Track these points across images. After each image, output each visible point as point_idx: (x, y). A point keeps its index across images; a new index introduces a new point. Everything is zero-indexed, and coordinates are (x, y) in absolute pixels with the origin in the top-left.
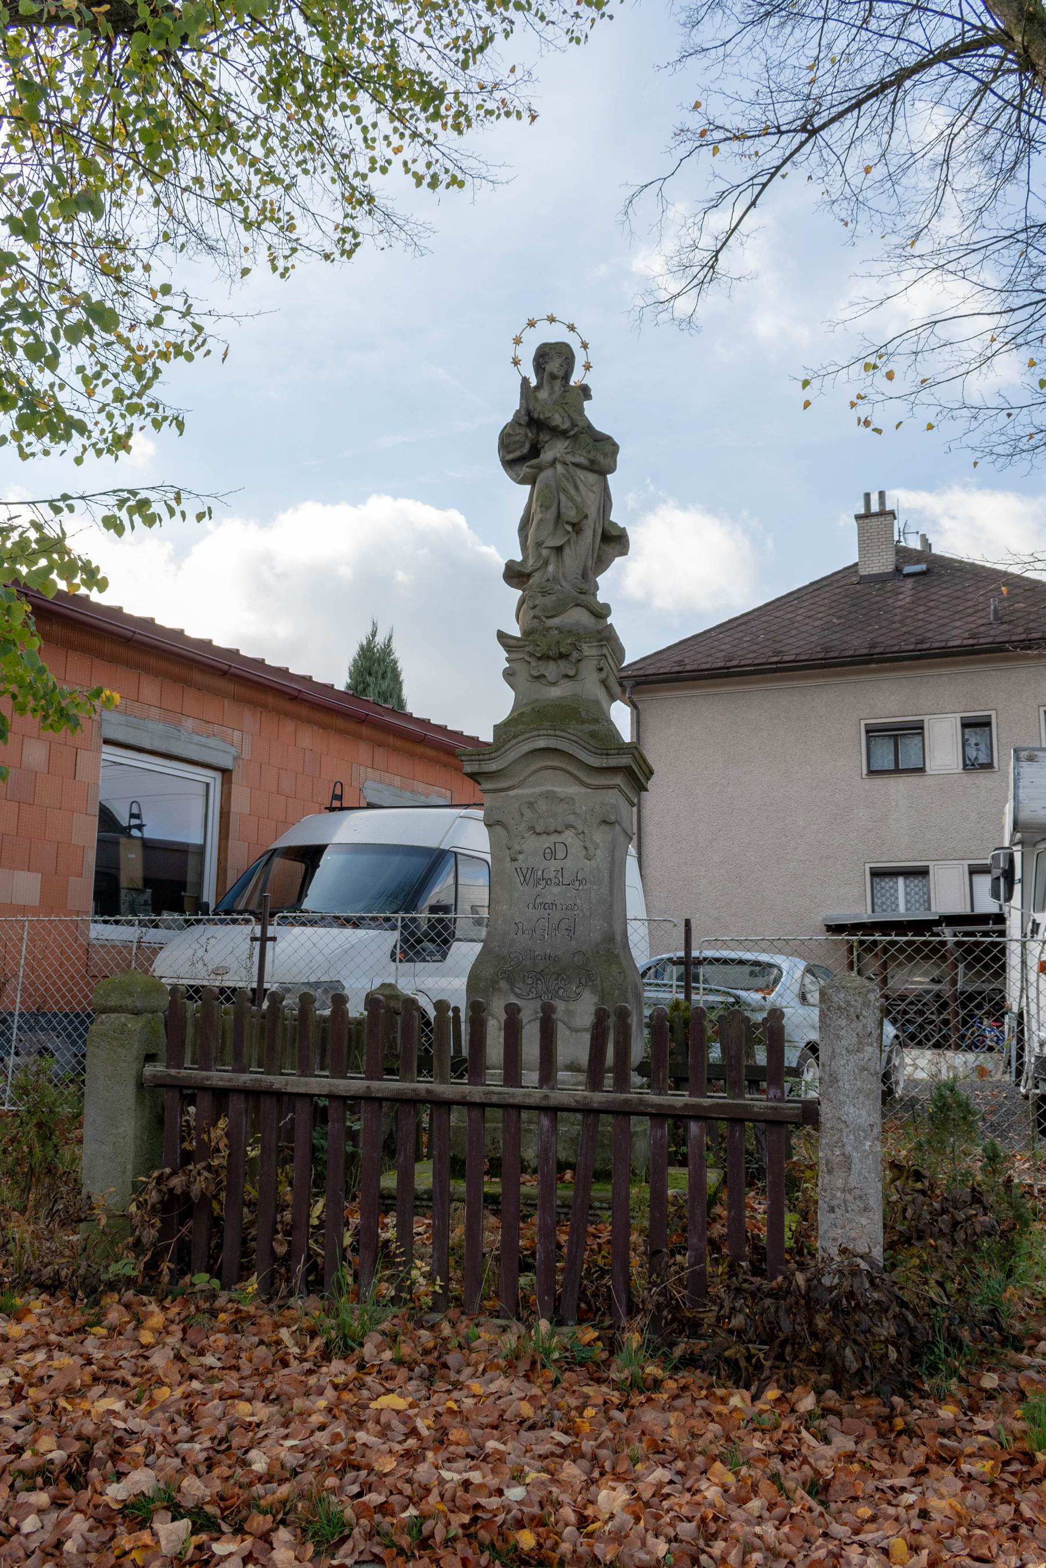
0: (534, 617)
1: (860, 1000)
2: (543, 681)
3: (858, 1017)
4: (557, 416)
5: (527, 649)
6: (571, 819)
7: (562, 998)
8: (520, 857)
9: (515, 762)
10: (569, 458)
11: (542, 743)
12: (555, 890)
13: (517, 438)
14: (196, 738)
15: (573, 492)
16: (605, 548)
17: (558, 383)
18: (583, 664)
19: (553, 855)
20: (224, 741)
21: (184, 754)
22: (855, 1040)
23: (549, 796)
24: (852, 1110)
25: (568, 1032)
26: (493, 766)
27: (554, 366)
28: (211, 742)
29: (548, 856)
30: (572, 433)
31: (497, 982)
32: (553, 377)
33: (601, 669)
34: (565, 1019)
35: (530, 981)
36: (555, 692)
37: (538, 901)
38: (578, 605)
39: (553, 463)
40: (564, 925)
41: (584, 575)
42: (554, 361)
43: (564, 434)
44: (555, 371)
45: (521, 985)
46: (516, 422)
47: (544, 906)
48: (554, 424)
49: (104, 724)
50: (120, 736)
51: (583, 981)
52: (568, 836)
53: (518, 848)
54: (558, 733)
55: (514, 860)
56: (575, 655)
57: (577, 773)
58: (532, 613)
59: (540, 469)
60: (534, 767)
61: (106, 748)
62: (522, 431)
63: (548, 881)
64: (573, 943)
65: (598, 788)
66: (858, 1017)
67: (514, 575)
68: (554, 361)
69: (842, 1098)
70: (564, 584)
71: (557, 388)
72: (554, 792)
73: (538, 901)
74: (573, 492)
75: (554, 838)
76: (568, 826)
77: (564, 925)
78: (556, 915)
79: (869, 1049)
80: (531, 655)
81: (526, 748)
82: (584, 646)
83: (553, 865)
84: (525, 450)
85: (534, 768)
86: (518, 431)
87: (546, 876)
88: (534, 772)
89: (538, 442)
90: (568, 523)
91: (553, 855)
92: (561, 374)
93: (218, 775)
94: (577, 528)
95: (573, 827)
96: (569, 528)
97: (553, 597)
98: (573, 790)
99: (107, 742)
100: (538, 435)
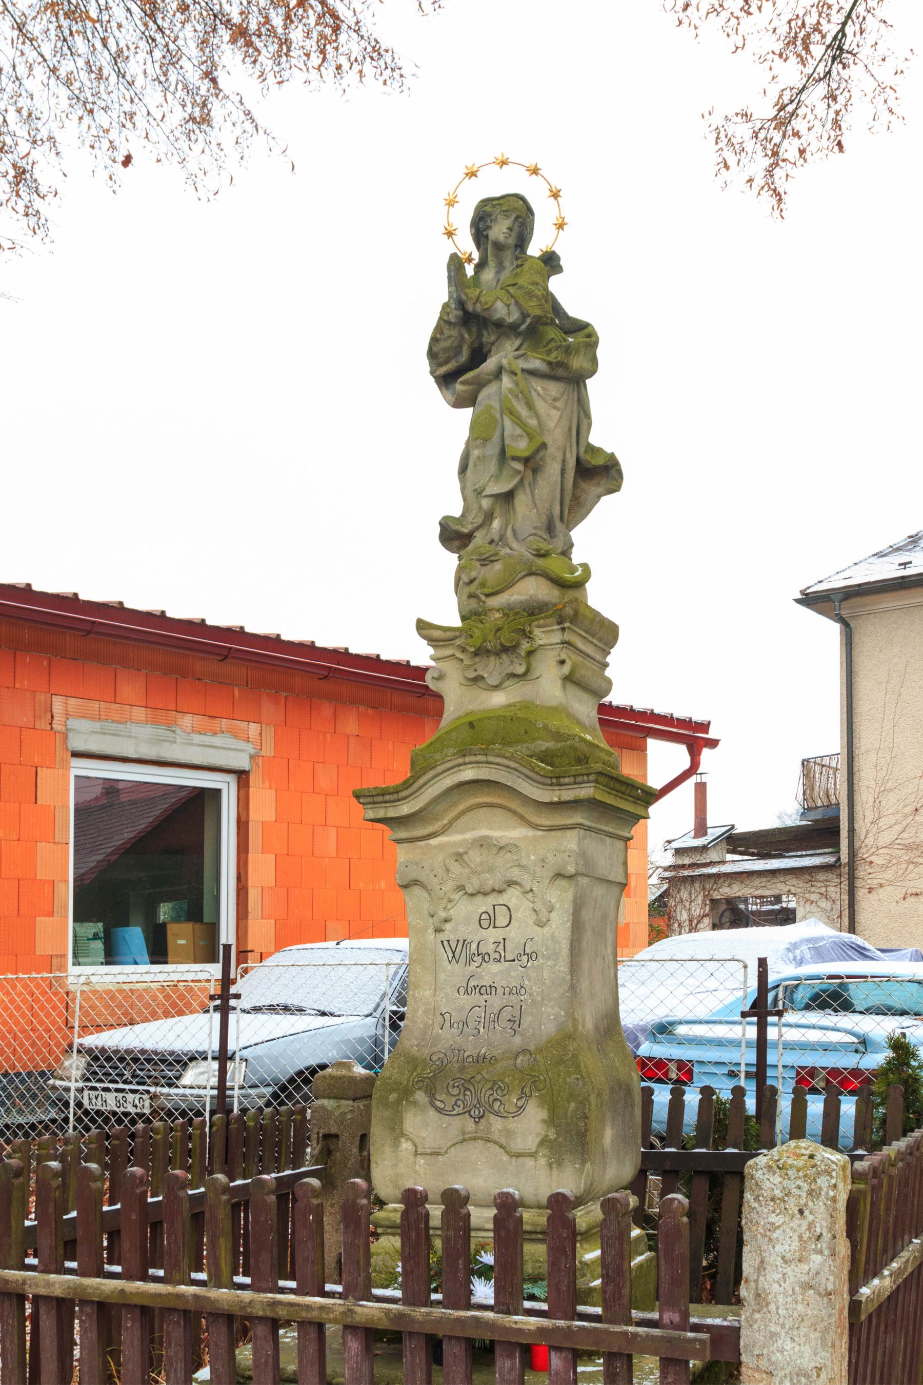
0: (471, 596)
1: (806, 1187)
2: (481, 684)
3: (801, 1212)
4: (499, 304)
5: (458, 642)
6: (515, 874)
7: (497, 1114)
8: (448, 926)
9: (436, 800)
10: (522, 364)
11: (468, 774)
12: (495, 968)
13: (448, 344)
14: (197, 738)
15: (523, 412)
16: (583, 485)
17: (508, 255)
18: (536, 659)
19: (492, 922)
20: (236, 737)
21: (183, 759)
22: (796, 1243)
23: (482, 843)
24: (788, 1345)
25: (505, 1158)
26: (405, 809)
27: (499, 231)
28: (217, 740)
29: (485, 924)
30: (523, 327)
31: (413, 1092)
32: (499, 247)
33: (562, 662)
34: (503, 1141)
35: (455, 1091)
36: (498, 699)
37: (472, 984)
38: (531, 574)
39: (498, 373)
40: (506, 1015)
41: (550, 529)
42: (502, 225)
43: (513, 329)
44: (501, 238)
45: (443, 1097)
46: (444, 322)
47: (479, 989)
48: (498, 316)
49: (70, 735)
50: (94, 747)
51: (527, 1090)
52: (512, 897)
53: (442, 914)
54: (490, 759)
55: (438, 930)
56: (525, 646)
57: (520, 810)
58: (467, 590)
59: (480, 384)
60: (461, 807)
61: (76, 762)
62: (454, 333)
63: (485, 957)
64: (518, 1040)
65: (551, 829)
66: (801, 1212)
67: (452, 535)
68: (502, 225)
69: (774, 1328)
70: (515, 545)
71: (507, 264)
72: (488, 837)
73: (472, 984)
74: (523, 412)
75: (492, 899)
76: (511, 883)
77: (506, 1015)
78: (496, 1002)
79: (817, 1259)
80: (463, 650)
81: (449, 781)
82: (537, 632)
83: (493, 935)
84: (464, 357)
85: (461, 807)
86: (447, 332)
87: (482, 950)
88: (463, 813)
89: (481, 346)
90: (514, 458)
91: (492, 922)
92: (511, 241)
93: (232, 779)
94: (532, 463)
95: (517, 883)
96: (519, 466)
97: (498, 566)
98: (516, 833)
99: (76, 755)
100: (480, 336)
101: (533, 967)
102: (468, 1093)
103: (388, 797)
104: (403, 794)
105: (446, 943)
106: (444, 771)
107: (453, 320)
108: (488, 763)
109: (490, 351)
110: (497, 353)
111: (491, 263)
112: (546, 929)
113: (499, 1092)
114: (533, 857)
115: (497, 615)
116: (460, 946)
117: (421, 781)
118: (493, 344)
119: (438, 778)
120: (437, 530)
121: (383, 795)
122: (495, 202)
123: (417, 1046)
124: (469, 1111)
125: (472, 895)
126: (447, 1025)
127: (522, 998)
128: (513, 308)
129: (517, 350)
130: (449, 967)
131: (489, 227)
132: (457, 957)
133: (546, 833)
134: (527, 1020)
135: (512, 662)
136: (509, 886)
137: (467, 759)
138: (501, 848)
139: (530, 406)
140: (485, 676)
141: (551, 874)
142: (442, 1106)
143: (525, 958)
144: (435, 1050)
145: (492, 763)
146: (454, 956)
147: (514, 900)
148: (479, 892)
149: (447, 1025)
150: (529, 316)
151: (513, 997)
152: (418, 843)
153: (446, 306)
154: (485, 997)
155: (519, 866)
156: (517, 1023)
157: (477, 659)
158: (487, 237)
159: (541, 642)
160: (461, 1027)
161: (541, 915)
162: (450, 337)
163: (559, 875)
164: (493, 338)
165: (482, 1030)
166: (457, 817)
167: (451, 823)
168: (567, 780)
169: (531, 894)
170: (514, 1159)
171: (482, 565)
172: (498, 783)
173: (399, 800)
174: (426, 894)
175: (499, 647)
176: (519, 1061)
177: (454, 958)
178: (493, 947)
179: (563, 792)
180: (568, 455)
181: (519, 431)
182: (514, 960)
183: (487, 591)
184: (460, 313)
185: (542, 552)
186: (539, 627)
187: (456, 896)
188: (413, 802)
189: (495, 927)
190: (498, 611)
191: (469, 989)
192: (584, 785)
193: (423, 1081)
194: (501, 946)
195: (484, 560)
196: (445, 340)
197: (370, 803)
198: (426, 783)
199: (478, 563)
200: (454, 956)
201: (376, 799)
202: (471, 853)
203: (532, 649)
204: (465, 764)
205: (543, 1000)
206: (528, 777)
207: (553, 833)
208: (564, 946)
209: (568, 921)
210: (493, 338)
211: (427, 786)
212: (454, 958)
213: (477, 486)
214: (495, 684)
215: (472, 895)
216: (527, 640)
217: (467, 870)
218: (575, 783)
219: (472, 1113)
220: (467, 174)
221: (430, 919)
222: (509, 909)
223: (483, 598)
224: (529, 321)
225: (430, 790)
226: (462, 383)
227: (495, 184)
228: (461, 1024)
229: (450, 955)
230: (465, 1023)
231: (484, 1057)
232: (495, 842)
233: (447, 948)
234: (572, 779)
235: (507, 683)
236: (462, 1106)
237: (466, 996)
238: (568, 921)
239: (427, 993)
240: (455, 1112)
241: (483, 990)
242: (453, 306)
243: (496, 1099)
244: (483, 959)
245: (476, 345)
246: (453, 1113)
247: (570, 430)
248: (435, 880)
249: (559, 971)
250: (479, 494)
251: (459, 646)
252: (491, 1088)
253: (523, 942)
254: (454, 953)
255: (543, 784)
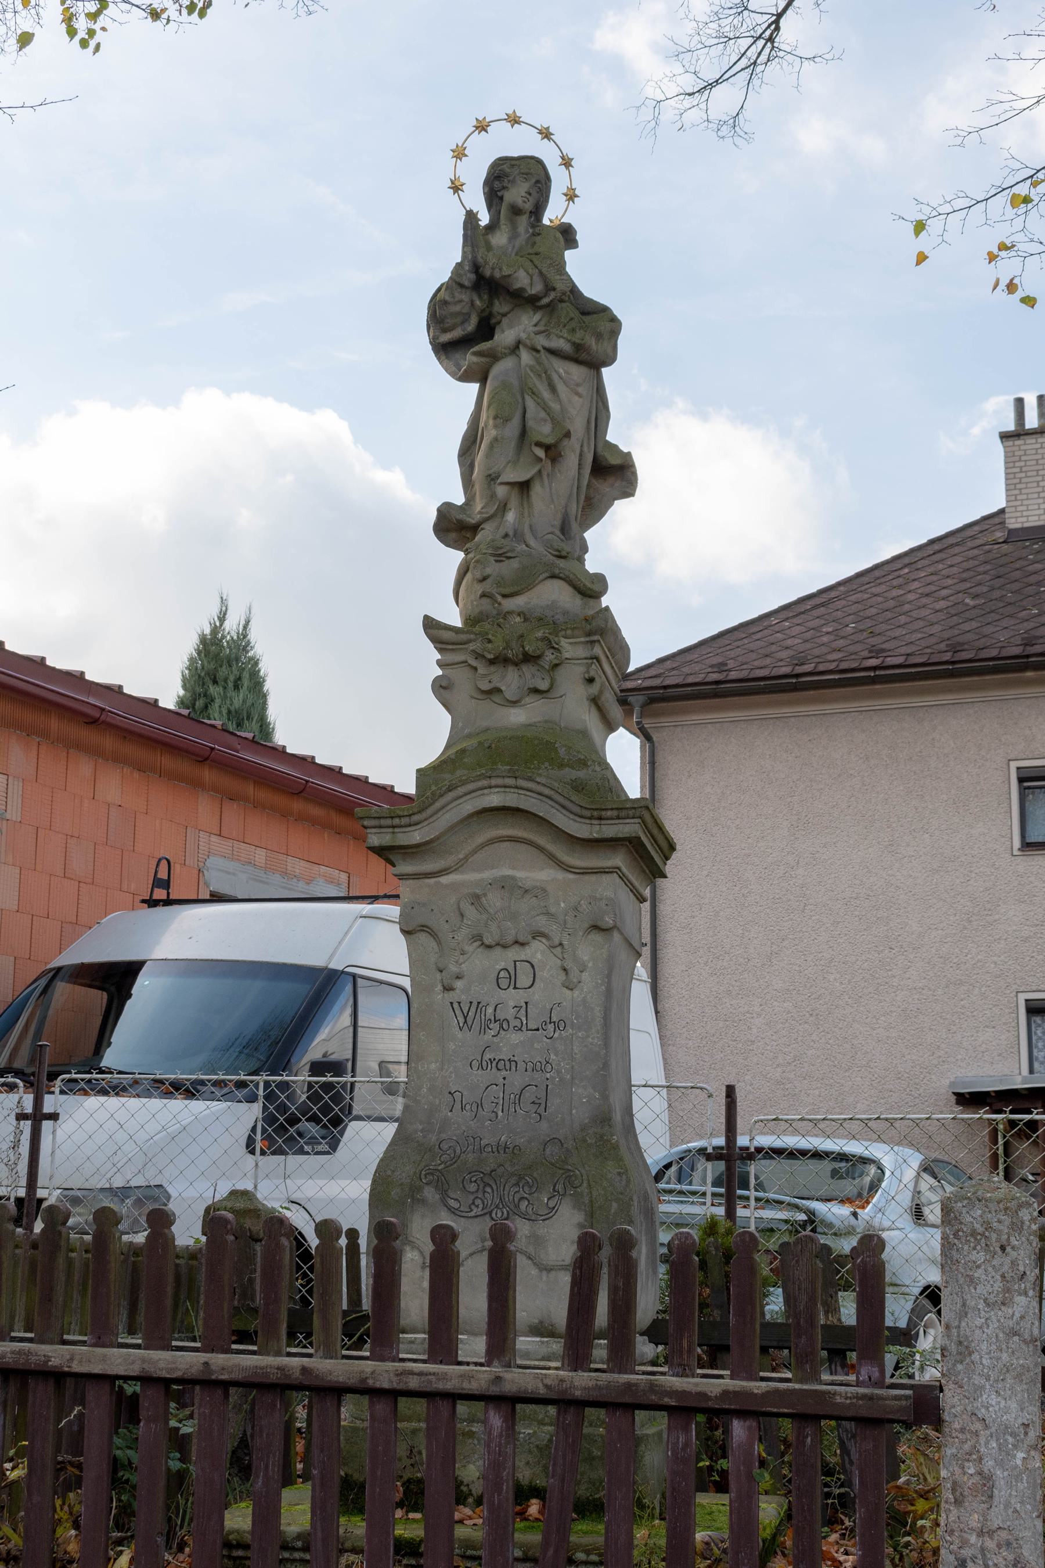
0: (484, 595)
1: (1007, 1220)
2: (497, 698)
3: (1003, 1248)
5: (472, 646)
6: (542, 923)
7: (524, 1216)
8: (459, 984)
9: (452, 828)
10: (541, 341)
11: (494, 799)
12: (515, 1038)
13: (457, 308)
15: (546, 395)
17: (523, 221)
18: (561, 673)
22: (998, 1286)
23: (506, 885)
24: (993, 1399)
25: (534, 1272)
26: (416, 836)
27: (517, 193)
29: (504, 983)
30: (545, 301)
31: (420, 1189)
32: (516, 211)
33: (591, 680)
34: (531, 1250)
35: (473, 1187)
36: (517, 717)
37: (487, 1056)
38: (553, 576)
39: (515, 349)
40: (529, 1095)
41: (564, 529)
42: (517, 187)
43: (532, 302)
44: (519, 202)
45: (458, 1194)
46: (455, 283)
47: (497, 1064)
51: (560, 1187)
52: (537, 951)
53: (454, 969)
55: (448, 989)
56: (549, 657)
57: (551, 847)
58: (479, 589)
59: (494, 357)
62: (465, 296)
63: (503, 1025)
64: (544, 1125)
66: (1003, 1248)
67: (452, 526)
68: (517, 187)
69: (978, 1380)
70: (532, 542)
72: (513, 878)
74: (546, 395)
75: (513, 953)
76: (537, 935)
77: (529, 1095)
78: (517, 1079)
79: (1021, 1300)
80: (478, 656)
81: (469, 806)
82: (564, 643)
83: (512, 998)
84: (471, 326)
85: (481, 839)
87: (500, 1015)
88: (482, 846)
89: (490, 315)
90: (538, 444)
92: (529, 206)
94: (553, 452)
96: (540, 453)
97: (515, 564)
98: (544, 875)
100: (491, 304)
101: (560, 1037)
102: (489, 1190)
103: (397, 821)
104: (415, 818)
105: (456, 1006)
106: (466, 794)
107: (466, 283)
108: (517, 787)
109: (499, 323)
110: (511, 327)
111: (503, 227)
112: (576, 993)
113: (526, 1189)
114: (562, 905)
115: (518, 619)
116: (473, 1009)
117: (438, 805)
118: (505, 315)
119: (458, 802)
120: (433, 515)
121: (392, 818)
122: (513, 162)
123: (422, 1131)
124: (490, 1213)
125: (489, 947)
126: (458, 1106)
127: (548, 1076)
128: (536, 278)
129: (535, 325)
130: (460, 1035)
131: (504, 188)
132: (470, 1023)
133: (578, 876)
134: (554, 1103)
135: (533, 676)
136: (533, 938)
137: (493, 782)
138: (526, 891)
139: (553, 389)
140: (503, 688)
141: (586, 925)
142: (456, 1205)
143: (551, 1027)
144: (444, 1136)
145: (522, 788)
146: (466, 1022)
147: (539, 956)
148: (498, 944)
149: (458, 1106)
150: (554, 289)
151: (537, 1075)
152: (427, 881)
153: (459, 265)
154: (504, 1073)
155: (548, 914)
156: (543, 1106)
157: (493, 668)
158: (501, 198)
159: (567, 655)
160: (475, 1110)
161: (571, 975)
162: (461, 301)
163: (595, 927)
164: (505, 309)
165: (500, 1114)
166: (474, 852)
167: (466, 858)
168: (609, 813)
169: (559, 949)
170: (544, 1273)
171: (496, 561)
172: (527, 812)
173: (410, 825)
174: (434, 944)
175: (521, 656)
176: (548, 1151)
177: (466, 1024)
178: (513, 1012)
179: (604, 828)
180: (585, 449)
181: (543, 414)
182: (538, 1030)
183: (506, 591)
184: (473, 276)
185: (564, 553)
186: (566, 637)
187: (469, 948)
188: (427, 829)
189: (515, 988)
190: (519, 615)
191: (484, 1063)
192: (628, 821)
193: (432, 1174)
194: (523, 1011)
195: (500, 555)
196: (455, 303)
197: (374, 827)
198: (443, 807)
199: (492, 559)
200: (466, 1022)
201: (383, 822)
202: (490, 895)
203: (557, 662)
204: (490, 787)
205: (573, 1078)
206: (564, 807)
207: (587, 877)
208: (598, 1014)
209: (601, 985)
210: (505, 309)
211: (444, 810)
212: (466, 1024)
213: (491, 472)
214: (514, 699)
215: (489, 947)
216: (552, 651)
217: (484, 917)
218: (618, 818)
219: (494, 1215)
220: (477, 128)
221: (438, 976)
222: (533, 966)
223: (499, 598)
224: (552, 295)
225: (447, 816)
226: (475, 354)
227: (520, 143)
228: (475, 1105)
229: (461, 1020)
230: (480, 1105)
231: (506, 1147)
232: (520, 884)
233: (458, 1012)
234: (615, 813)
235: (527, 700)
236: (481, 1206)
237: (480, 1072)
238: (601, 985)
239: (433, 1065)
240: (472, 1214)
241: (501, 1065)
242: (467, 268)
243: (522, 1198)
244: (501, 1027)
245: (485, 314)
246: (470, 1215)
247: (588, 422)
248: (447, 926)
249: (592, 1044)
250: (492, 480)
251: (473, 651)
252: (517, 1184)
253: (548, 1007)
254: (465, 1018)
255: (581, 817)
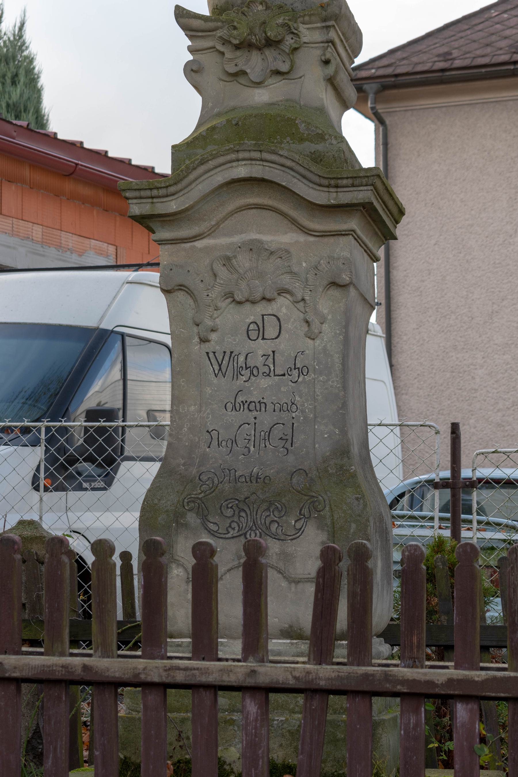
2: (242, 80)
5: (219, 33)
6: (286, 281)
8: (213, 336)
9: (204, 198)
11: (242, 171)
12: (264, 382)
18: (301, 57)
23: (254, 248)
25: (284, 584)
26: (173, 206)
29: (253, 335)
31: (183, 515)
33: (327, 62)
34: (281, 565)
35: (229, 512)
36: (261, 97)
37: (240, 399)
40: (277, 432)
47: (248, 405)
52: (282, 306)
53: (209, 323)
54: (266, 156)
55: (204, 340)
56: (289, 41)
57: (293, 213)
63: (253, 371)
64: (291, 458)
65: (324, 234)
73: (240, 399)
75: (261, 308)
76: (283, 291)
77: (277, 432)
78: (266, 419)
80: (225, 42)
81: (220, 178)
82: (302, 28)
83: (261, 347)
85: (230, 207)
87: (251, 363)
98: (288, 238)
101: (304, 382)
102: (243, 514)
103: (155, 192)
104: (172, 189)
105: (211, 355)
106: (216, 167)
108: (262, 160)
112: (318, 342)
113: (276, 513)
114: (304, 265)
115: (260, 8)
116: (227, 358)
117: (192, 177)
119: (209, 174)
121: (151, 189)
123: (184, 465)
124: (245, 534)
125: (240, 303)
126: (215, 443)
127: (294, 415)
130: (215, 381)
132: (224, 370)
133: (317, 239)
134: (299, 439)
135: (275, 59)
136: (279, 294)
137: (241, 155)
138: (272, 253)
140: (248, 71)
141: (325, 282)
142: (215, 528)
143: (295, 373)
144: (203, 469)
145: (266, 161)
146: (220, 369)
147: (284, 310)
148: (247, 300)
149: (215, 443)
151: (284, 415)
152: (183, 245)
154: (255, 413)
155: (291, 272)
156: (289, 442)
157: (238, 53)
159: (305, 39)
160: (229, 445)
161: (313, 327)
163: (334, 284)
165: (252, 448)
166: (225, 219)
168: (345, 182)
169: (302, 304)
170: (293, 585)
172: (271, 182)
173: (167, 196)
174: (190, 301)
175: (263, 41)
176: (294, 480)
177: (221, 372)
178: (261, 359)
179: (341, 195)
182: (284, 375)
186: (303, 23)
187: (222, 304)
188: (182, 199)
189: (263, 339)
191: (237, 405)
193: (194, 502)
194: (271, 359)
197: (136, 198)
198: (196, 179)
200: (220, 369)
201: (143, 193)
202: (240, 257)
203: (297, 46)
204: (238, 160)
205: (315, 417)
206: (304, 177)
207: (326, 240)
208: (337, 360)
209: (340, 334)
211: (197, 182)
212: (221, 372)
214: (258, 81)
215: (240, 303)
216: (291, 36)
217: (235, 276)
218: (353, 186)
219: (248, 536)
221: (195, 329)
222: (279, 319)
225: (200, 187)
228: (230, 442)
229: (216, 368)
230: (234, 441)
231: (257, 478)
232: (266, 247)
233: (213, 360)
234: (350, 181)
235: (270, 81)
236: (237, 528)
237: (234, 413)
238: (340, 334)
239: (192, 408)
240: (229, 535)
241: (252, 407)
243: (273, 521)
244: (252, 373)
246: (227, 536)
248: (202, 285)
249: (332, 386)
251: (221, 37)
252: (268, 509)
253: (293, 355)
254: (220, 366)
255: (320, 185)
